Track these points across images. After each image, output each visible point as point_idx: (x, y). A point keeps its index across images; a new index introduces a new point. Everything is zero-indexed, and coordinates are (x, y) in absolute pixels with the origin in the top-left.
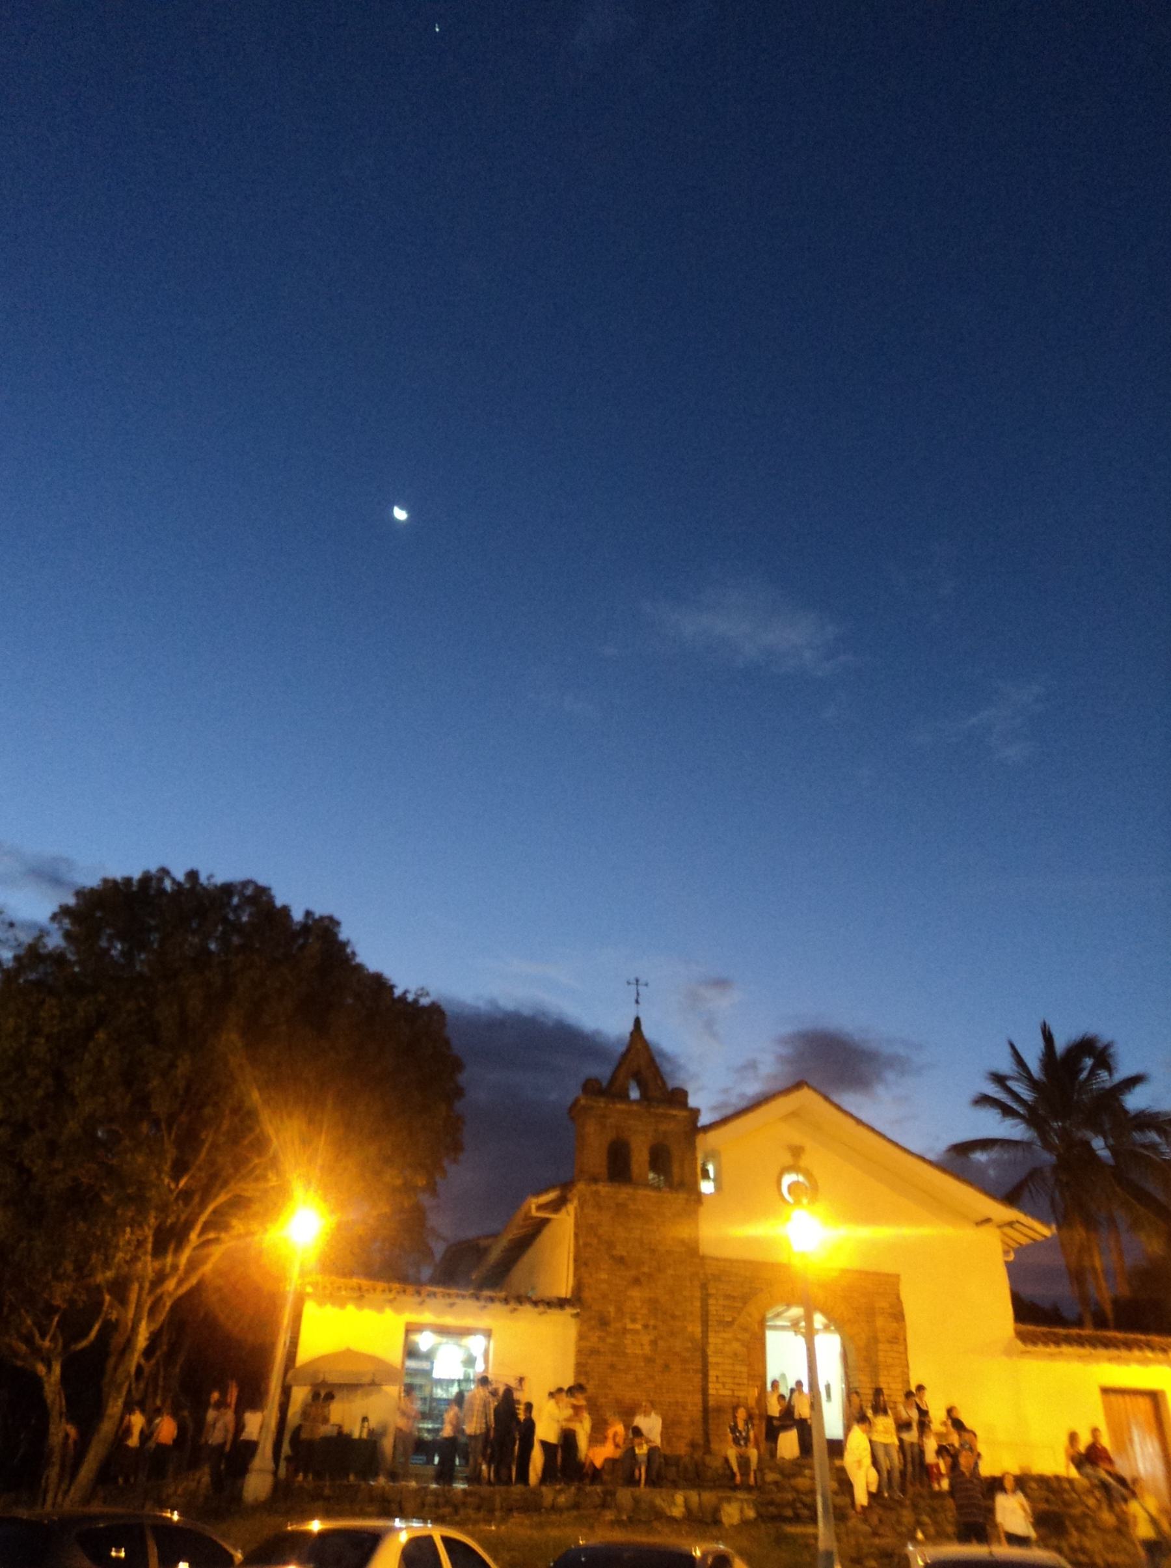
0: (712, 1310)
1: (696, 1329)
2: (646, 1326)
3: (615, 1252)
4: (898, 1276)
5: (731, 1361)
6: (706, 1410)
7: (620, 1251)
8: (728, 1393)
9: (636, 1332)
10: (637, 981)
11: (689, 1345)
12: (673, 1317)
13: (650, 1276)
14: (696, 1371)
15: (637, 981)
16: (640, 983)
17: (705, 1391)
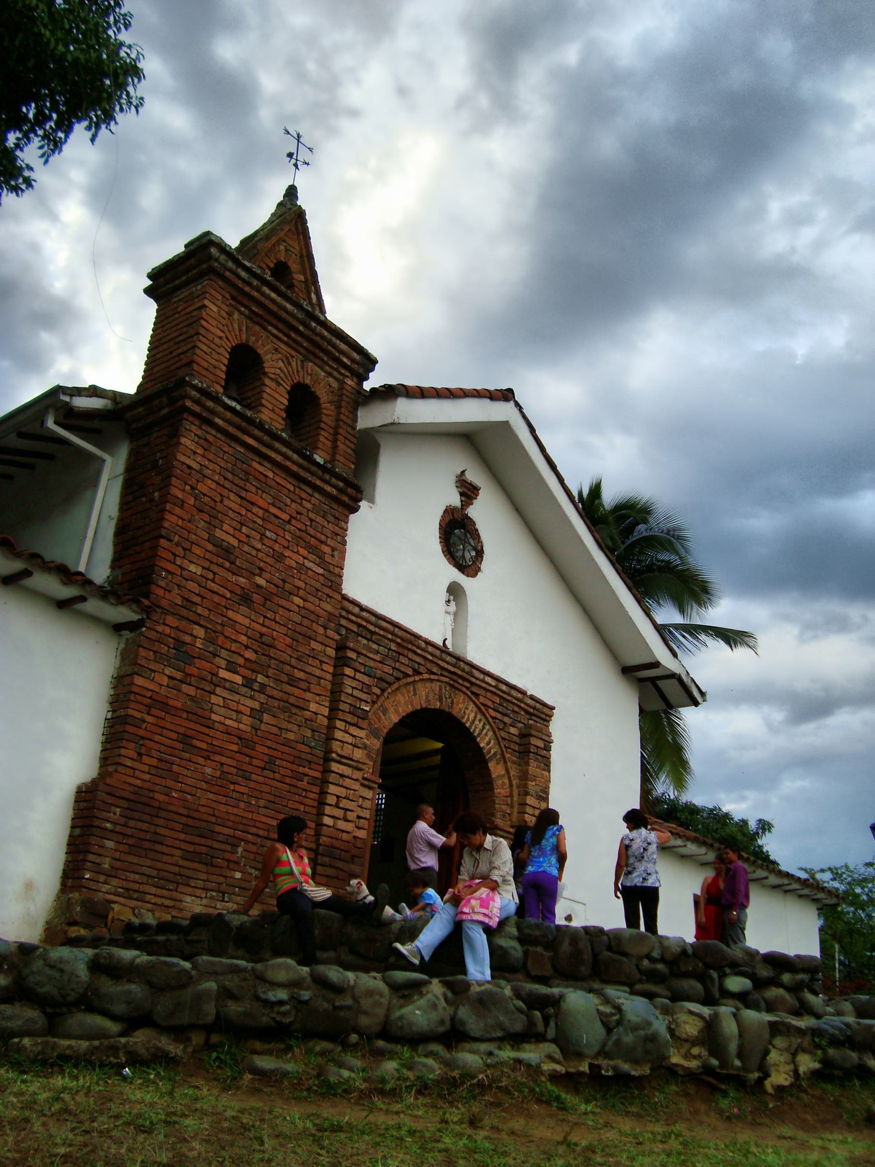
1: (319, 708)
2: (248, 683)
3: (218, 533)
4: (553, 708)
11: (309, 733)
12: (292, 681)
14: (313, 781)
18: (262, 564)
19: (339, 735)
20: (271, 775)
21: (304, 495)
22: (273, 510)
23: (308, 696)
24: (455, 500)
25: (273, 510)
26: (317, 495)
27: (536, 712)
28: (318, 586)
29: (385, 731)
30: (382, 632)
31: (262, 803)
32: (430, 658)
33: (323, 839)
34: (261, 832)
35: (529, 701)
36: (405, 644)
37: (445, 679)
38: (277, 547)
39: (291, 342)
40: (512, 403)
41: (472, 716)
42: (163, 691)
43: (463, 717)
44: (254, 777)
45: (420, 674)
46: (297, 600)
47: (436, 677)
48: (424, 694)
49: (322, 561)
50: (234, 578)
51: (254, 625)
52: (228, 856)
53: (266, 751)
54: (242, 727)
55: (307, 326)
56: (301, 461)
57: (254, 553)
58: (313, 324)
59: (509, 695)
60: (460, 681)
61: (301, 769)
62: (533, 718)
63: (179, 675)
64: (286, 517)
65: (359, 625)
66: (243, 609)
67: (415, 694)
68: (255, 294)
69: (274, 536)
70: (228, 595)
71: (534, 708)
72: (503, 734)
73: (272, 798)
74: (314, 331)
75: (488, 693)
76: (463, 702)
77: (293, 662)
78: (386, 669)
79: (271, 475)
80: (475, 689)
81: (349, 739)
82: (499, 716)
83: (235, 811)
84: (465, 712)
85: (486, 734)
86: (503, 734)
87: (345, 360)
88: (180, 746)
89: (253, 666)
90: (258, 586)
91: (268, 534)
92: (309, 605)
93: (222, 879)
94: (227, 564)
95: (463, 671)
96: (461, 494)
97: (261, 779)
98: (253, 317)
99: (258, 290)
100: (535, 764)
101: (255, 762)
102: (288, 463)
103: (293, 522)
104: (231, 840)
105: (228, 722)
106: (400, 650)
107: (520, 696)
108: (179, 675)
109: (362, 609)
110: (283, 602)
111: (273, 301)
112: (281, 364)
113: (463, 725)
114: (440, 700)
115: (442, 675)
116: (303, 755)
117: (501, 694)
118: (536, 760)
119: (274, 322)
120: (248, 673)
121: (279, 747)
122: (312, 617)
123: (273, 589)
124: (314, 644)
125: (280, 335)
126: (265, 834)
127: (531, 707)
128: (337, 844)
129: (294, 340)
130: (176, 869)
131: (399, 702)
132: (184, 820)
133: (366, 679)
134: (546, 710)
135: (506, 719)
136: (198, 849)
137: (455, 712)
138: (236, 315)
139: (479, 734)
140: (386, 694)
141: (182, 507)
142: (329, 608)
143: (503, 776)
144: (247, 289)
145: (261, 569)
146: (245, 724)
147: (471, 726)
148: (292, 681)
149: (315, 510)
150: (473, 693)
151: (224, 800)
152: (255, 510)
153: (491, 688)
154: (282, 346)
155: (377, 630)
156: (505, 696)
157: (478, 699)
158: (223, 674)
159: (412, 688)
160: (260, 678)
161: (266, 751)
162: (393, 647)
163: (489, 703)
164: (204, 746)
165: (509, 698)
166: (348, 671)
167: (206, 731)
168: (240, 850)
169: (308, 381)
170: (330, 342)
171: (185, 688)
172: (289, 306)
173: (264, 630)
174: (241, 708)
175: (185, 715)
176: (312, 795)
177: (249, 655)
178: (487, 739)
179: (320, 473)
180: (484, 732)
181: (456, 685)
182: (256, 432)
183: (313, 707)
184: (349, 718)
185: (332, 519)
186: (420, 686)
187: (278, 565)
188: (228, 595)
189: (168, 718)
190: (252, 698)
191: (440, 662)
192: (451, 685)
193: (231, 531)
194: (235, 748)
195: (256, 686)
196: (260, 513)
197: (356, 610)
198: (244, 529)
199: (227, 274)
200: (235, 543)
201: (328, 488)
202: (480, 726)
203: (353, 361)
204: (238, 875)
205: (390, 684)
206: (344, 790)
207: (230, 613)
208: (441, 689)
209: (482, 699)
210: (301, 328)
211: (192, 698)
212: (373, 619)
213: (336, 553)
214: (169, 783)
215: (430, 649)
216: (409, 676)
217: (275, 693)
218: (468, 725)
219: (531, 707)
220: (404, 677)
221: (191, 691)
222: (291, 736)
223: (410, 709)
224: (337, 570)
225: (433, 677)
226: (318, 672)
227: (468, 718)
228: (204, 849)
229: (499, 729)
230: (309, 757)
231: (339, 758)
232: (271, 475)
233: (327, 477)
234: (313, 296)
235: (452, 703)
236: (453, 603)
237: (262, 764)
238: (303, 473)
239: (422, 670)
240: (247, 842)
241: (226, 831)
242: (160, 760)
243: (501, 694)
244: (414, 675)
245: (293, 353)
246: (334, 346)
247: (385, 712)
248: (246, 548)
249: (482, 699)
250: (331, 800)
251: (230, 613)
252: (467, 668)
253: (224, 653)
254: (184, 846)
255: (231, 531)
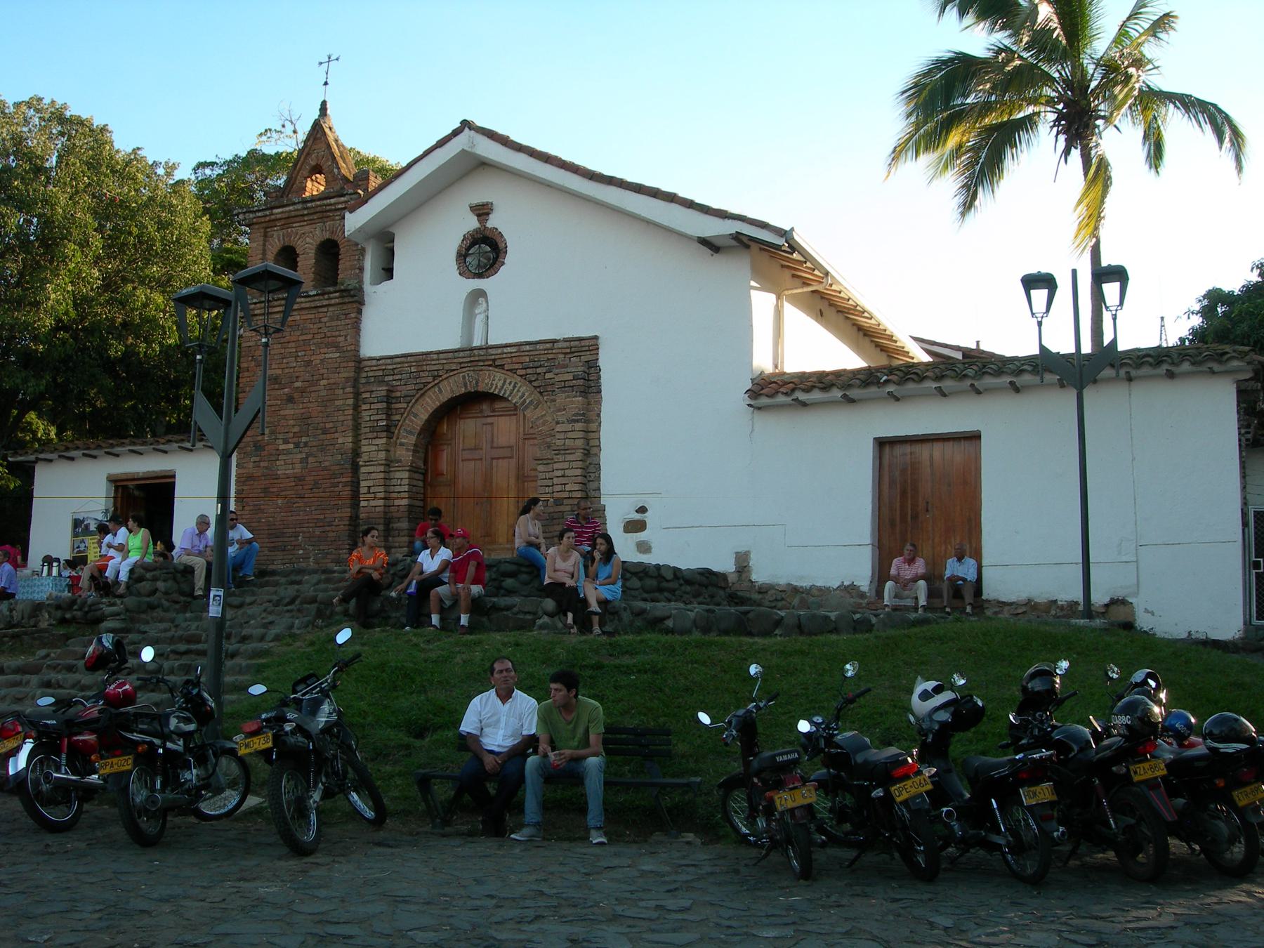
0: (366, 416)
2: (297, 445)
5: (382, 468)
6: (354, 519)
7: (274, 371)
8: (381, 502)
9: (288, 452)
10: (329, 58)
12: (325, 431)
13: (302, 391)
14: (345, 484)
15: (329, 58)
16: (332, 58)
17: (355, 502)
18: (297, 374)
19: (364, 449)
20: (317, 490)
21: (321, 315)
22: (301, 338)
23: (336, 435)
24: (472, 223)
25: (301, 338)
26: (330, 309)
27: (573, 350)
28: (337, 365)
29: (419, 428)
30: (399, 366)
31: (313, 508)
32: (445, 362)
33: (362, 516)
34: (311, 525)
35: (560, 345)
36: (421, 363)
37: (464, 370)
38: (306, 359)
39: (309, 222)
40: (467, 129)
41: (500, 384)
42: (251, 471)
43: (490, 389)
44: (306, 496)
45: (441, 376)
46: (323, 382)
47: (455, 372)
48: (448, 388)
49: (336, 346)
50: (281, 392)
51: (297, 411)
52: (294, 543)
53: (312, 478)
54: (295, 471)
55: (307, 208)
56: (307, 299)
57: (292, 370)
58: (309, 205)
59: (536, 350)
60: (482, 364)
61: (336, 480)
62: (576, 354)
63: (257, 459)
64: (310, 337)
65: (384, 370)
66: (290, 405)
67: (440, 390)
68: (273, 217)
69: (303, 353)
70: (279, 402)
71: (571, 348)
72: (535, 384)
73: (319, 503)
74: (312, 207)
75: (514, 359)
76: (489, 377)
77: (324, 420)
78: (409, 387)
79: (298, 318)
80: (497, 364)
81: (374, 448)
82: (529, 371)
83: (298, 517)
84: (492, 384)
85: (518, 391)
86: (535, 384)
87: (340, 206)
88: (262, 495)
89: (299, 435)
90: (297, 388)
91: (300, 354)
92: (332, 381)
93: (291, 557)
94: (277, 386)
95: (479, 355)
96: (479, 216)
97: (311, 495)
98: (283, 227)
99: (272, 214)
100: (564, 395)
101: (305, 487)
102: (303, 305)
103: (316, 336)
104: (294, 534)
105: (287, 472)
106: (420, 369)
107: (548, 346)
108: (257, 459)
109: (378, 360)
110: (314, 389)
111: (282, 212)
112: (308, 240)
113: (492, 394)
114: (465, 385)
115: (461, 368)
116: (337, 472)
117: (526, 353)
118: (566, 392)
119: (293, 220)
120: (295, 440)
121: (319, 473)
122: (334, 387)
123: (306, 384)
124: (337, 403)
125: (302, 224)
126: (314, 525)
127: (568, 348)
128: (371, 515)
129: (311, 220)
130: (265, 558)
131: (427, 403)
132: (266, 532)
133: (379, 406)
134: (587, 343)
135: (539, 370)
136: (277, 544)
137: (482, 388)
138: (275, 233)
139: (511, 393)
140: (410, 405)
141: (248, 371)
142: (346, 375)
143: (545, 415)
144: (268, 218)
145: (297, 377)
146: (298, 469)
147: (500, 391)
148: (325, 431)
149: (332, 319)
150: (496, 366)
151: (289, 514)
152: (290, 345)
153: (513, 355)
154: (307, 228)
155: (395, 366)
156: (531, 353)
157: (503, 369)
158: (281, 447)
159: (437, 389)
160: (304, 439)
161: (312, 478)
162: (413, 370)
163: (516, 366)
164: (275, 490)
165: (537, 353)
166: (364, 407)
167: (276, 481)
168: (300, 538)
169: (327, 236)
170: (326, 205)
171: (262, 464)
172: (291, 208)
173: (303, 411)
174: (294, 461)
175: (263, 478)
176: (346, 493)
177: (296, 429)
178: (520, 394)
179: (321, 297)
180: (516, 390)
181: (476, 368)
182: (276, 303)
183: (340, 441)
184: (370, 435)
185: (343, 317)
186: (445, 382)
187: (309, 369)
188: (279, 402)
189: (256, 483)
190: (300, 452)
191: (455, 361)
192: (474, 370)
193: (276, 366)
194: (293, 484)
195: (302, 445)
196: (293, 345)
197: (374, 362)
198: (284, 361)
199: (255, 220)
200: (279, 372)
201: (333, 302)
202: (511, 388)
203: (346, 202)
204: (301, 552)
205: (414, 396)
206: (372, 481)
207: (282, 413)
208: (464, 377)
209: (506, 367)
210: (306, 212)
211: (267, 468)
212: (389, 361)
213: (349, 337)
214: (260, 515)
215: (442, 356)
216: (430, 383)
217: (314, 444)
218: (496, 393)
219: (568, 348)
220: (425, 386)
221: (265, 464)
222: (327, 464)
223: (438, 404)
224: (349, 349)
225: (451, 374)
226: (341, 418)
227: (496, 387)
228: (280, 544)
229: (530, 382)
230: (341, 471)
231: (363, 464)
232: (298, 318)
233: (326, 296)
234: (336, 170)
235: (477, 383)
236: (485, 305)
237: (310, 487)
238: (313, 305)
239: (441, 373)
240: (304, 532)
241: (290, 530)
242: (254, 505)
243: (526, 353)
244: (434, 380)
245: (314, 226)
246: (331, 205)
247: (416, 416)
248: (287, 371)
249: (506, 367)
250: (363, 490)
251: (282, 413)
252: (481, 352)
253: (281, 436)
254: (268, 545)
255: (276, 366)
